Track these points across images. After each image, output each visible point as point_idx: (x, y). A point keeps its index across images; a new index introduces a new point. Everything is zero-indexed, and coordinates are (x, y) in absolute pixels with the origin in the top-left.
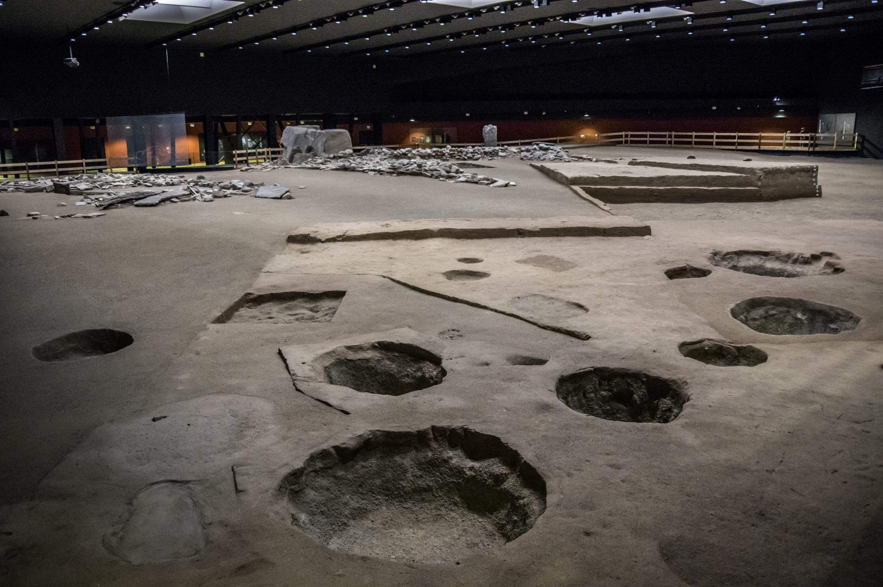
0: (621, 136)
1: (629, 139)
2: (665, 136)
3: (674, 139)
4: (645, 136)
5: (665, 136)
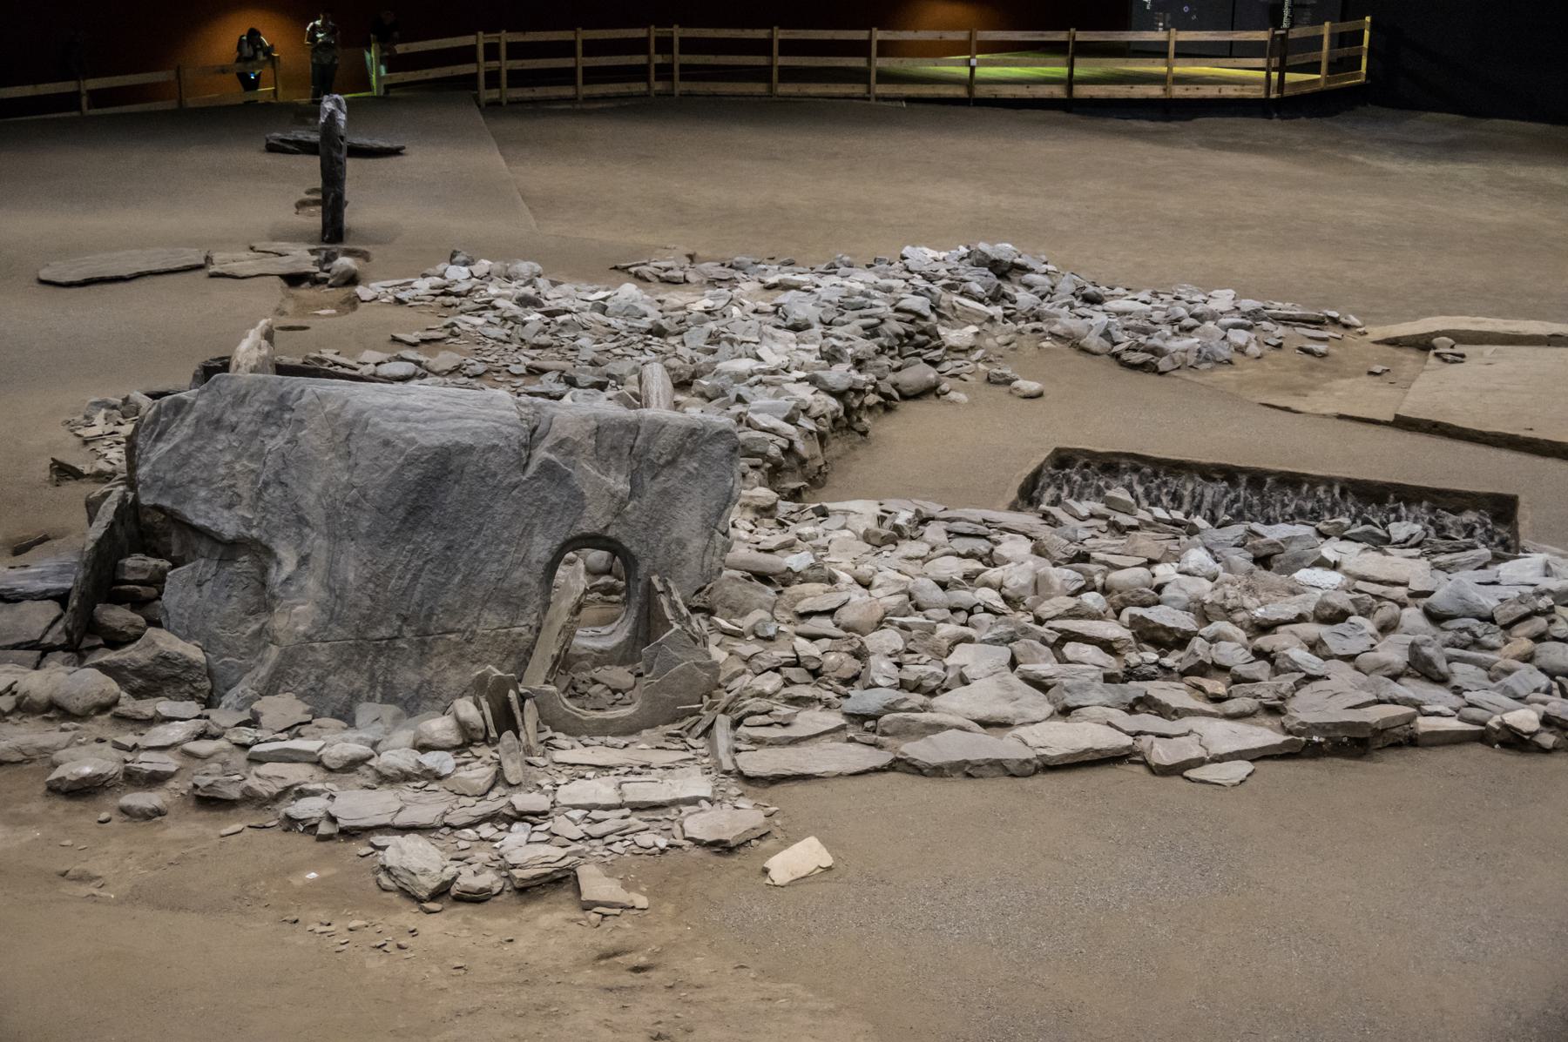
0: (468, 55)
1: (506, 65)
2: (639, 46)
3: (680, 59)
4: (567, 49)
5: (639, 46)
